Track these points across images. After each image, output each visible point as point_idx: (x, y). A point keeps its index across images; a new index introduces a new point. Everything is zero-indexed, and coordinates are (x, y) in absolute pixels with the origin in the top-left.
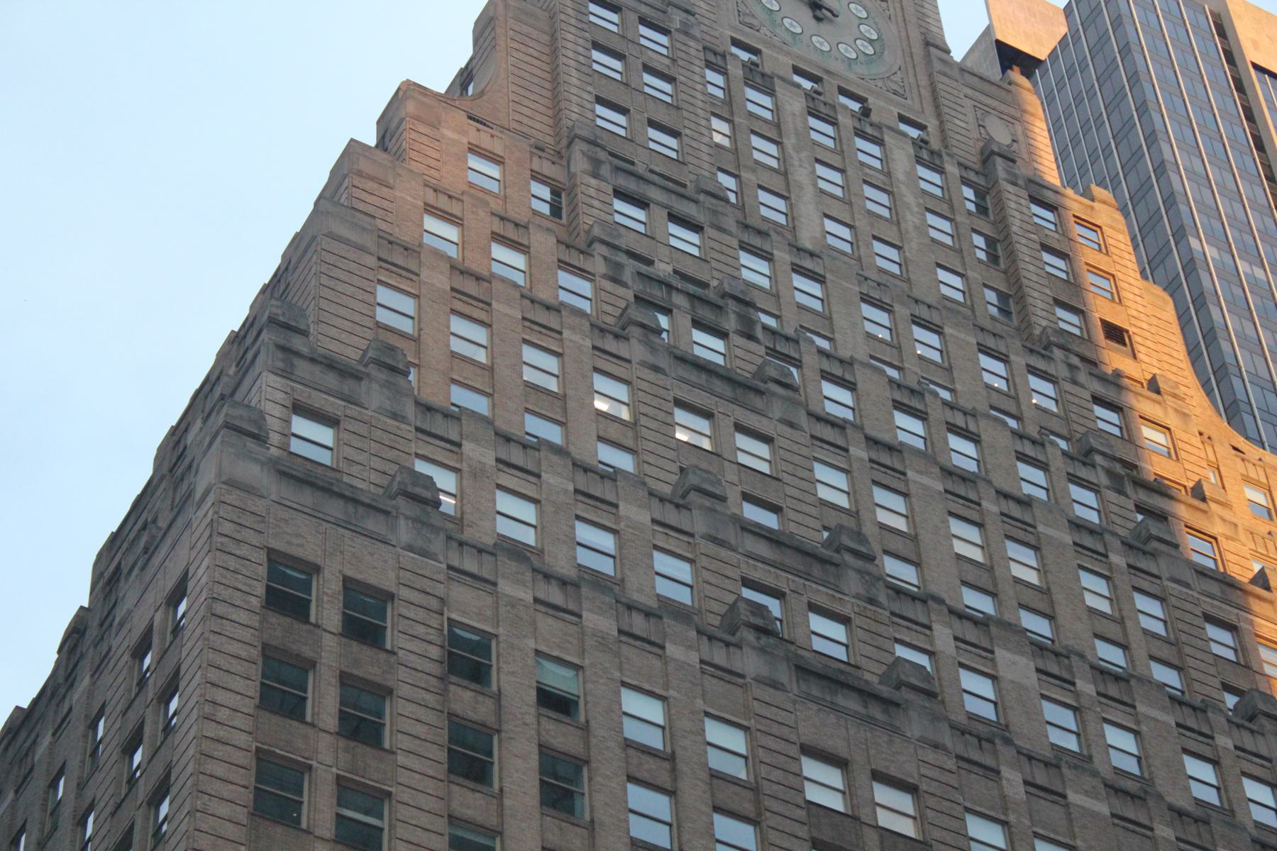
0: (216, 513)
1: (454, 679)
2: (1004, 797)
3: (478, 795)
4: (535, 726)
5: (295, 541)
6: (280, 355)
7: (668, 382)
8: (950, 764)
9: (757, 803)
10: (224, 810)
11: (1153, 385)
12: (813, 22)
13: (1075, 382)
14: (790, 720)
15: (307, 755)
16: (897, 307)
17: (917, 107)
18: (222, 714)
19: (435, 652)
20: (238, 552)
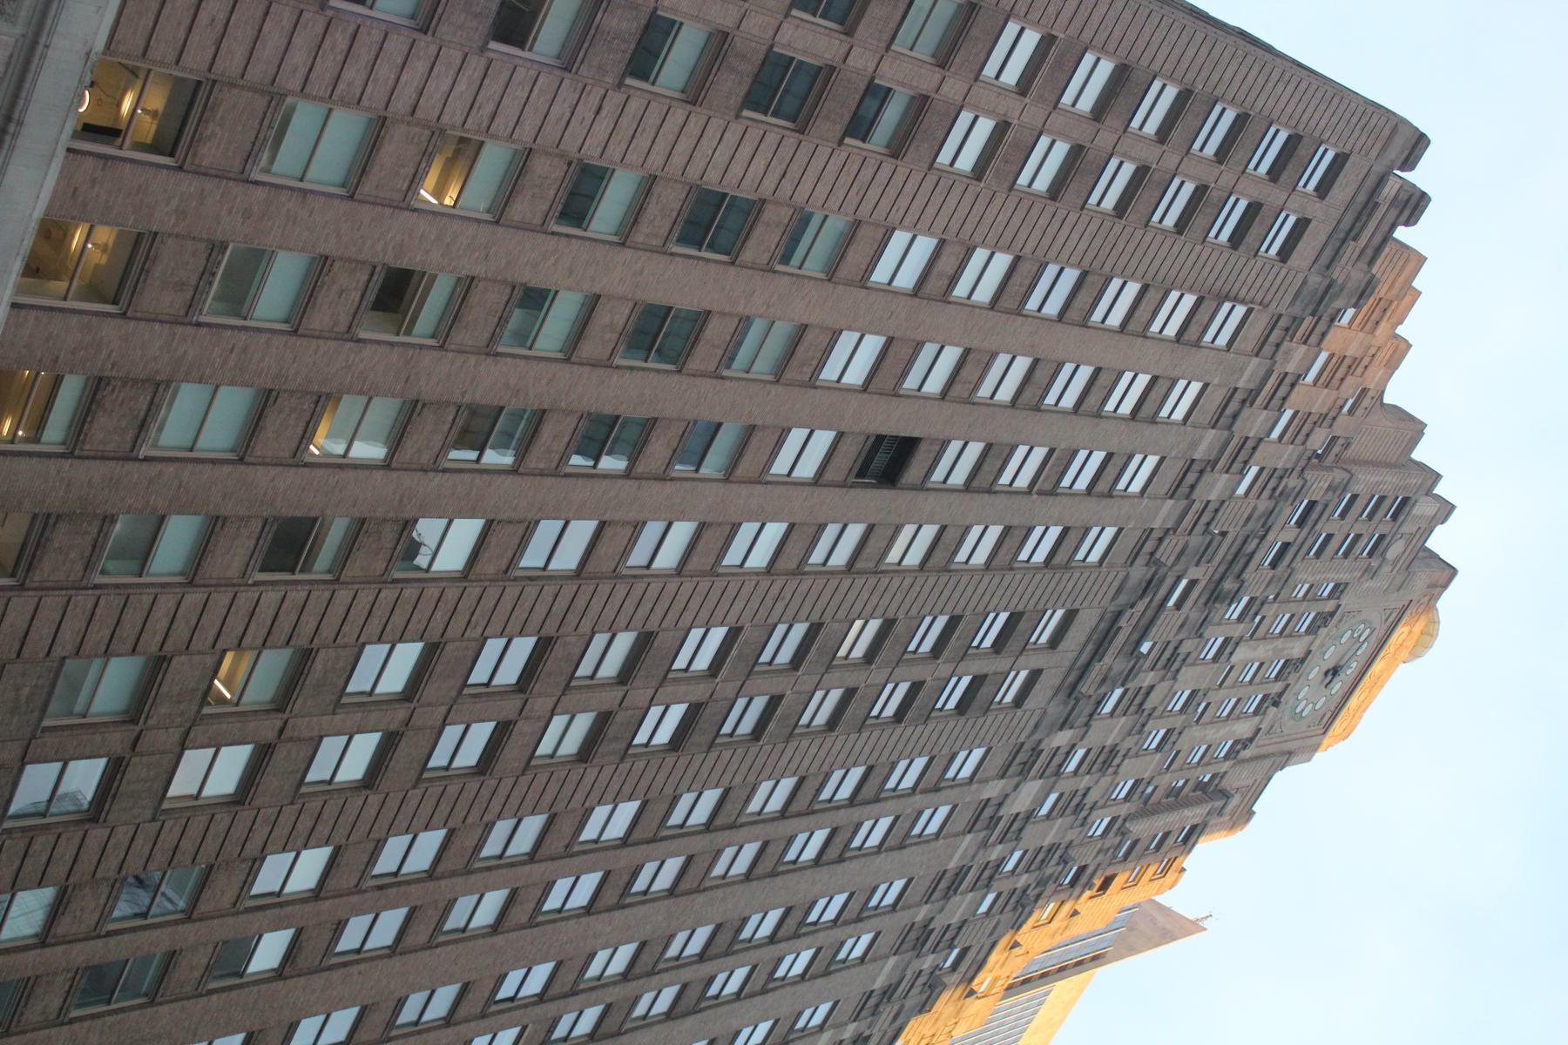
2: (986, 781)
6: (1406, 198)
7: (1238, 528)
8: (1022, 739)
9: (1059, 567)
11: (1075, 913)
12: (1325, 669)
13: (1098, 853)
14: (1095, 603)
16: (1183, 717)
17: (1261, 743)
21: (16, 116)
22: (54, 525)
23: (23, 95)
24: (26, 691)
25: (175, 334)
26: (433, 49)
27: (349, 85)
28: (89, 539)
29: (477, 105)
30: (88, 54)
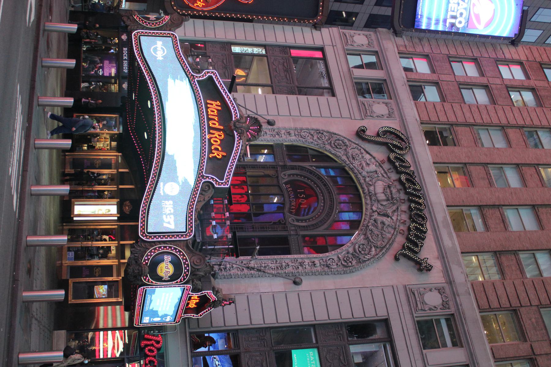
21: (409, 136)
22: (500, 257)
23: (408, 131)
24: (533, 320)
25: (491, 191)
26: (500, 107)
27: (486, 119)
28: (515, 261)
29: (525, 119)
30: (416, 119)
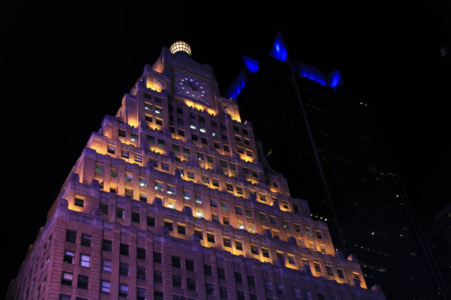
0: (57, 223)
1: (103, 251)
3: (107, 274)
4: (119, 259)
5: (73, 227)
10: (56, 285)
15: (73, 271)
18: (56, 265)
19: (100, 246)
20: (61, 231)
